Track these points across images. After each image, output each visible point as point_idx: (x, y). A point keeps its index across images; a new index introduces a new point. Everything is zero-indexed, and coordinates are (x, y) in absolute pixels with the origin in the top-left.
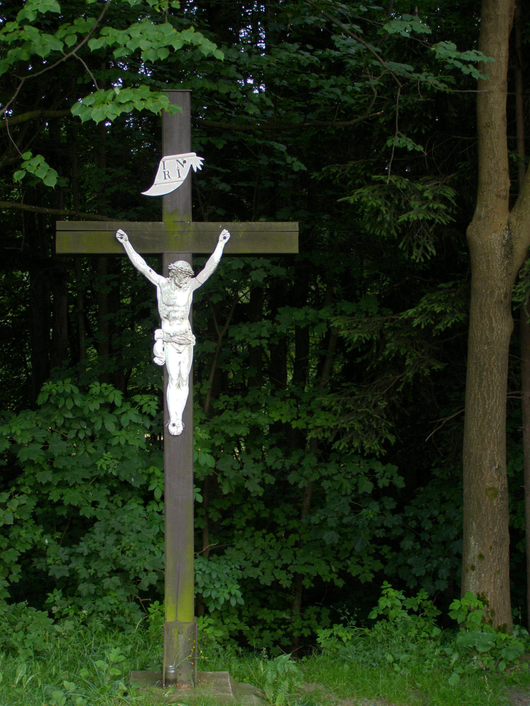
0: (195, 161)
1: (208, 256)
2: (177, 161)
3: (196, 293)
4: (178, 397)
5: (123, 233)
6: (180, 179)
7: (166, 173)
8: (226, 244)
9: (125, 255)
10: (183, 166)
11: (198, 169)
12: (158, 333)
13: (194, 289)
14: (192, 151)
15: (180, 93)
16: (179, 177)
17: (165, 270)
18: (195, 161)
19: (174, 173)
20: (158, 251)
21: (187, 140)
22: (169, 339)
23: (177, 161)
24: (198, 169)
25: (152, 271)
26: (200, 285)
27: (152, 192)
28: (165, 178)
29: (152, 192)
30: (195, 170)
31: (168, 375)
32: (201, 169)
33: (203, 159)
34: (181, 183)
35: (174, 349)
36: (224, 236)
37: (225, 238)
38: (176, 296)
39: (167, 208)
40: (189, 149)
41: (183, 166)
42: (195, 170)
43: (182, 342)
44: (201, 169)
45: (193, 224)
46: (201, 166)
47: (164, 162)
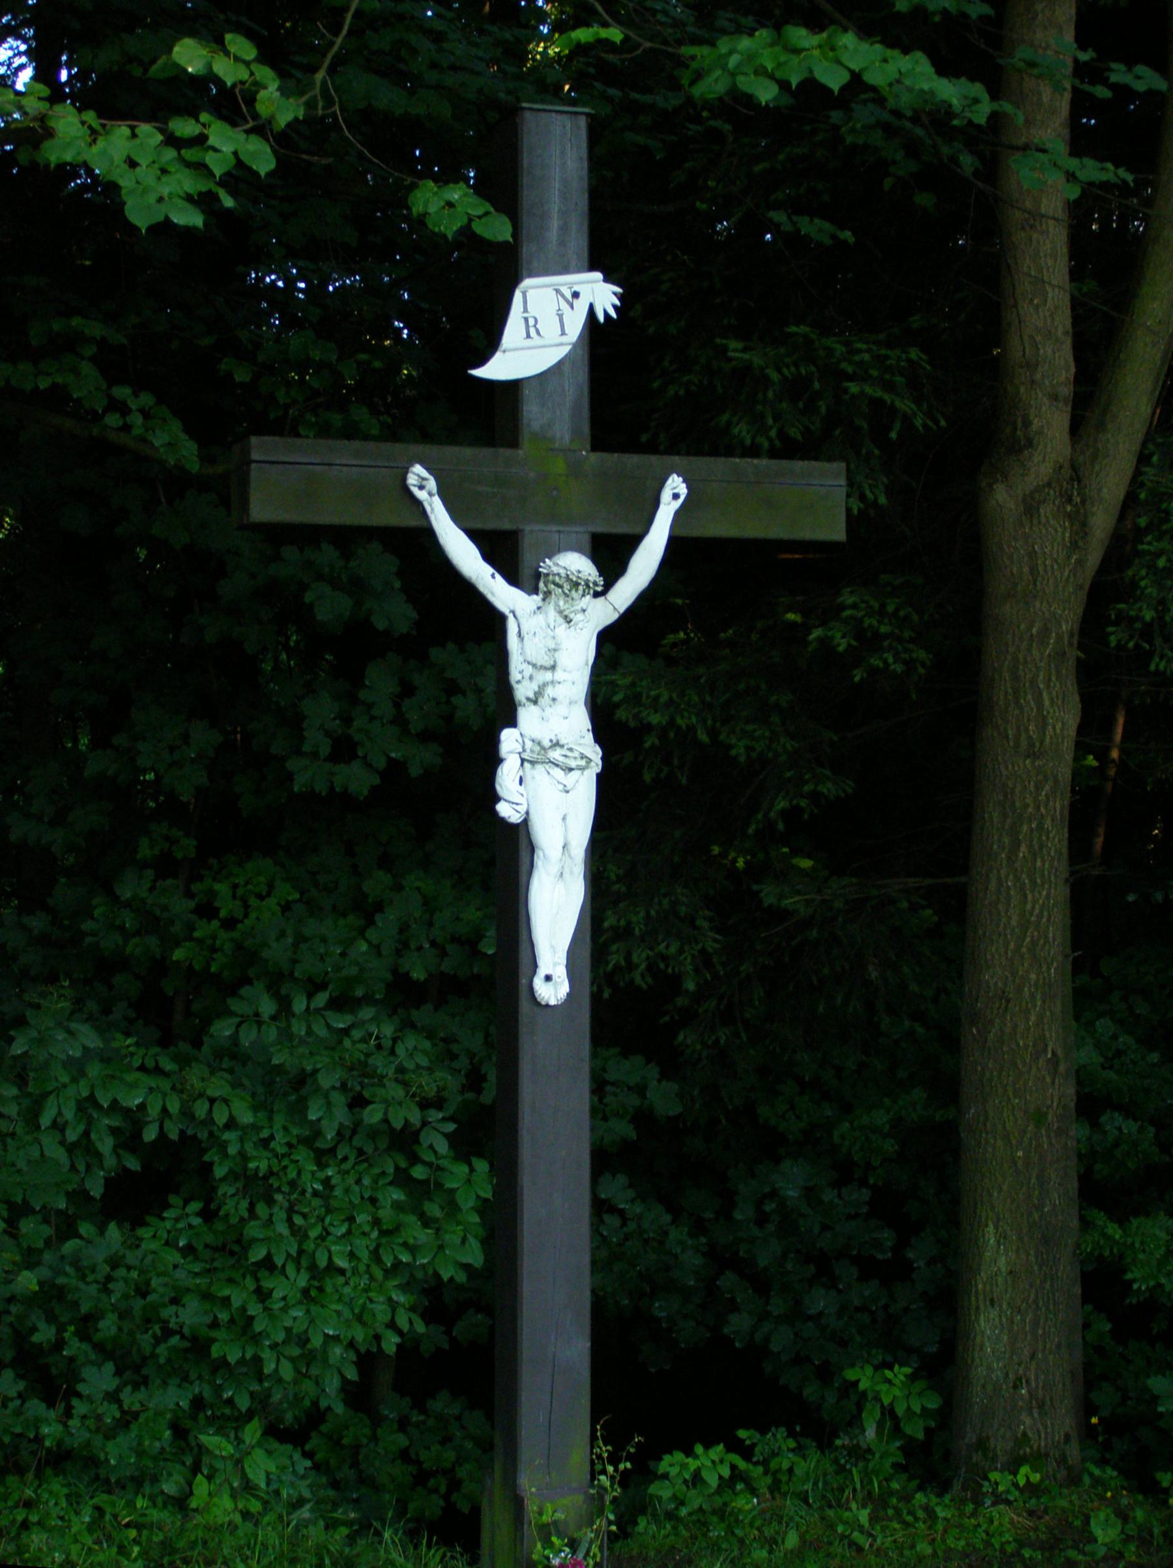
0: (601, 294)
1: (632, 542)
2: (557, 291)
3: (606, 637)
4: (555, 904)
5: (424, 473)
6: (564, 339)
7: (531, 322)
8: (678, 514)
9: (428, 534)
10: (572, 307)
11: (606, 314)
12: (509, 739)
13: (600, 628)
14: (592, 268)
15: (565, 117)
16: (563, 333)
17: (526, 573)
18: (601, 294)
19: (547, 323)
20: (507, 525)
21: (578, 242)
22: (538, 756)
23: (557, 291)
24: (606, 314)
25: (497, 576)
26: (616, 616)
27: (495, 369)
28: (528, 336)
29: (495, 369)
30: (601, 318)
31: (532, 848)
32: (613, 314)
33: (619, 290)
34: (565, 350)
35: (549, 784)
36: (674, 490)
37: (676, 496)
38: (554, 639)
39: (533, 413)
40: (586, 264)
41: (572, 307)
42: (601, 318)
43: (573, 764)
44: (613, 314)
45: (594, 457)
46: (615, 307)
47: (524, 294)
